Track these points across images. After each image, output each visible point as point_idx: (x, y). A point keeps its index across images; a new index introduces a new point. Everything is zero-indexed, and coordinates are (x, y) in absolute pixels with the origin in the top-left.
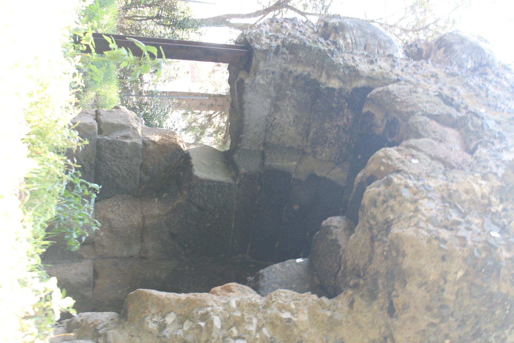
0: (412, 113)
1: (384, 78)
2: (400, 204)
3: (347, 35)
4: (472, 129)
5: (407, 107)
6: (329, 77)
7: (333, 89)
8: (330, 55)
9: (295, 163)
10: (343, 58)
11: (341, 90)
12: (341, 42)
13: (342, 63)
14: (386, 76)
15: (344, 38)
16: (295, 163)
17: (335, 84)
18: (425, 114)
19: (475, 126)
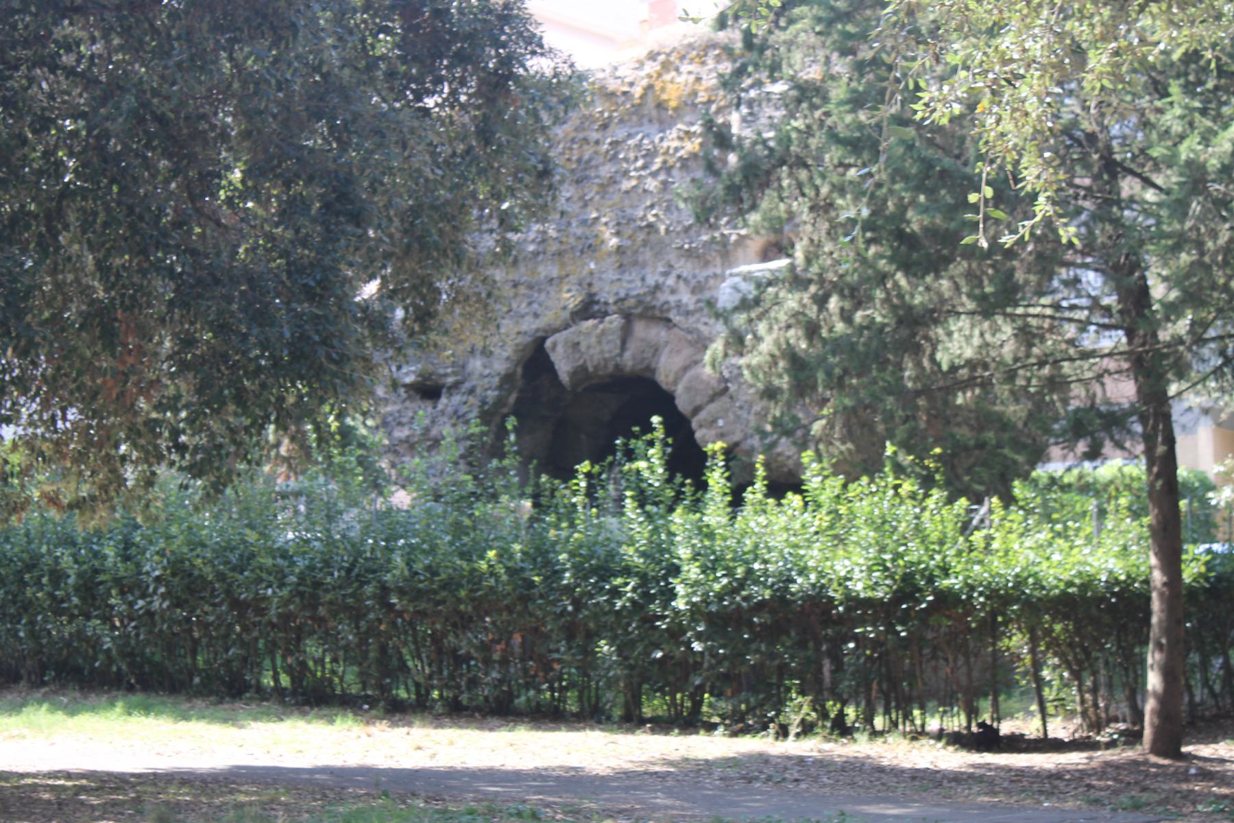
0: (617, 366)
1: (523, 350)
2: (776, 461)
3: (441, 371)
4: (639, 310)
5: (606, 367)
6: (505, 405)
7: (518, 401)
8: (486, 407)
9: (583, 437)
10: (486, 390)
11: (521, 391)
12: (450, 380)
13: (496, 393)
14: (521, 348)
15: (446, 375)
16: (583, 437)
17: (512, 399)
18: (621, 355)
19: (636, 307)
